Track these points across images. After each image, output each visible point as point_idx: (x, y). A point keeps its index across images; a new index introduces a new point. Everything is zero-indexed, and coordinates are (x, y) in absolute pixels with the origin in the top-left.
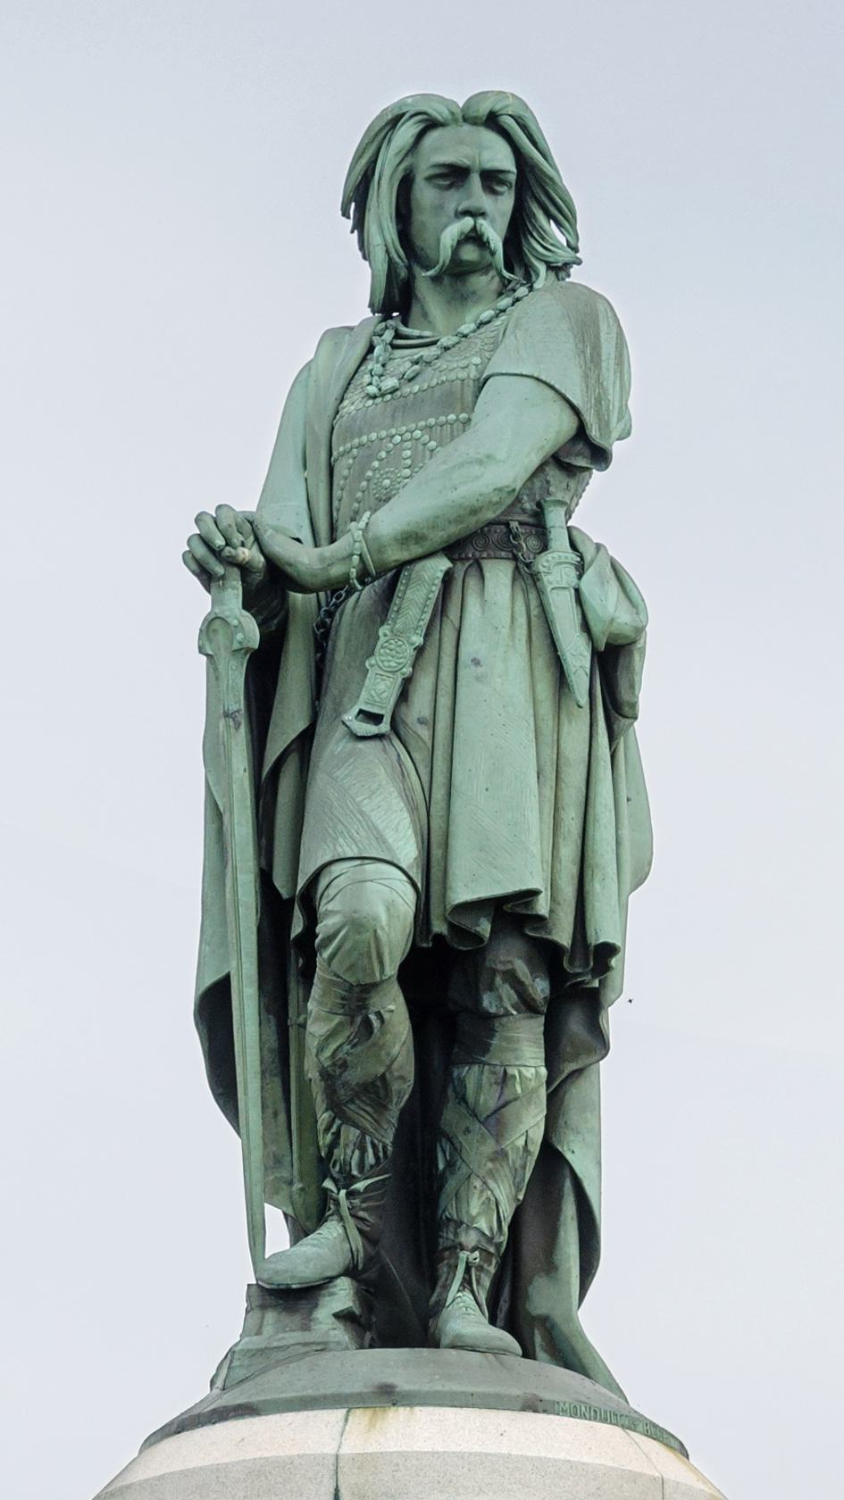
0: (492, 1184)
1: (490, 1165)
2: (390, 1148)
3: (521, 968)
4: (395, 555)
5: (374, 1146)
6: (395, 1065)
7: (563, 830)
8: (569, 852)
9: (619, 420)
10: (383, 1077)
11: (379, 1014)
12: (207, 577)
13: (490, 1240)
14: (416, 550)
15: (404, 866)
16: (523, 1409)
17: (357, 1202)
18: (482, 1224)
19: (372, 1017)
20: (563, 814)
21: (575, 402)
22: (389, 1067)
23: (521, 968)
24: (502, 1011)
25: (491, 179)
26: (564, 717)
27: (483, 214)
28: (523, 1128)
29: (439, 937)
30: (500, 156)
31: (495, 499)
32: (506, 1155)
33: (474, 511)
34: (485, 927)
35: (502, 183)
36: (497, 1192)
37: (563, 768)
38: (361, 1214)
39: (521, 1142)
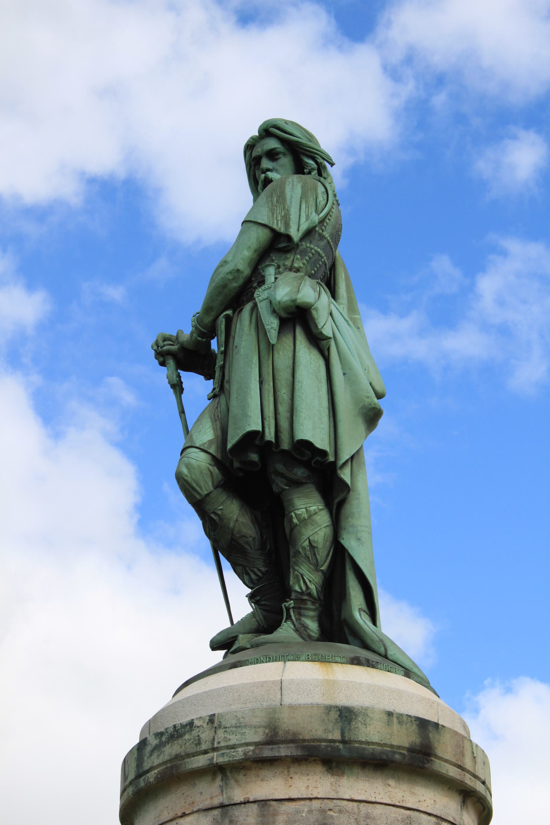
0: (297, 568)
1: (294, 559)
2: (263, 569)
3: (280, 467)
4: (208, 320)
5: (253, 571)
6: (235, 532)
7: (280, 399)
8: (283, 410)
9: (307, 220)
10: (232, 539)
11: (214, 513)
12: (163, 364)
13: (302, 593)
14: (213, 314)
15: (197, 445)
16: (230, 669)
17: (258, 598)
18: (297, 588)
19: (213, 516)
20: (278, 393)
21: (263, 222)
22: (233, 534)
23: (280, 467)
24: (280, 490)
25: (272, 155)
26: (275, 352)
27: (268, 170)
28: (305, 537)
29: (239, 469)
30: (272, 144)
31: (230, 277)
32: (299, 552)
33: (224, 286)
34: (254, 457)
35: (278, 154)
36: (301, 571)
37: (276, 373)
38: (263, 603)
39: (307, 543)
